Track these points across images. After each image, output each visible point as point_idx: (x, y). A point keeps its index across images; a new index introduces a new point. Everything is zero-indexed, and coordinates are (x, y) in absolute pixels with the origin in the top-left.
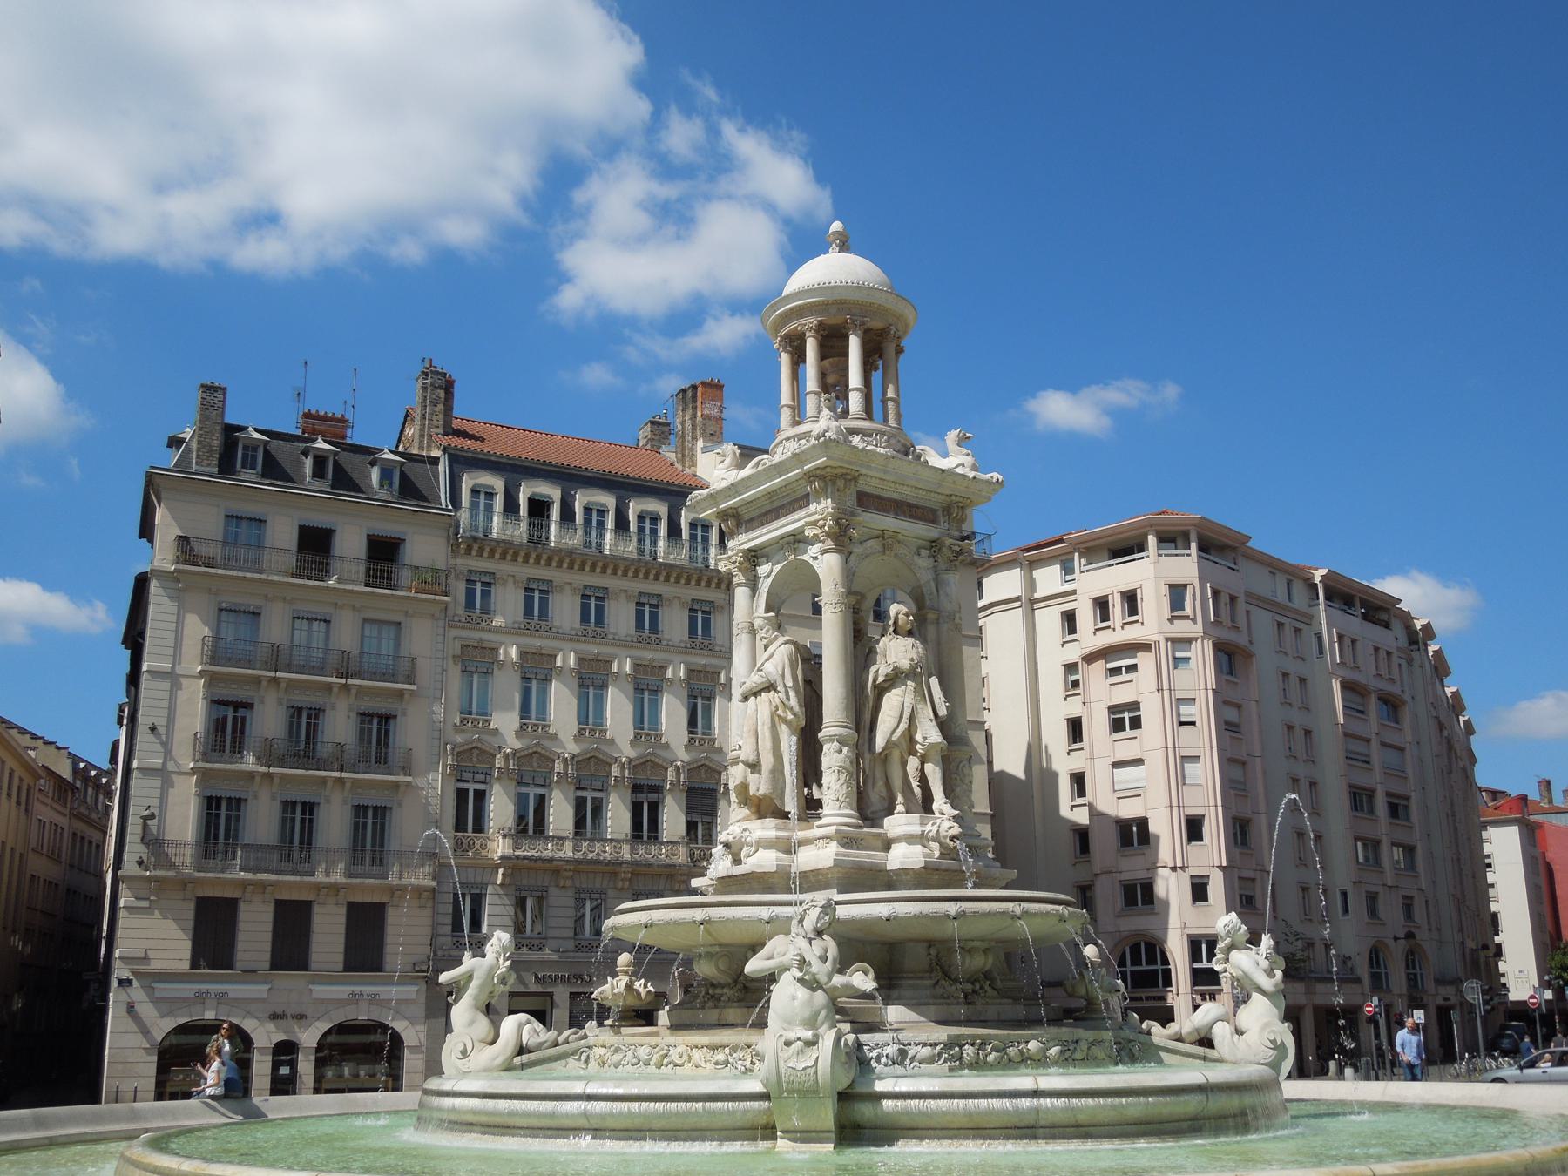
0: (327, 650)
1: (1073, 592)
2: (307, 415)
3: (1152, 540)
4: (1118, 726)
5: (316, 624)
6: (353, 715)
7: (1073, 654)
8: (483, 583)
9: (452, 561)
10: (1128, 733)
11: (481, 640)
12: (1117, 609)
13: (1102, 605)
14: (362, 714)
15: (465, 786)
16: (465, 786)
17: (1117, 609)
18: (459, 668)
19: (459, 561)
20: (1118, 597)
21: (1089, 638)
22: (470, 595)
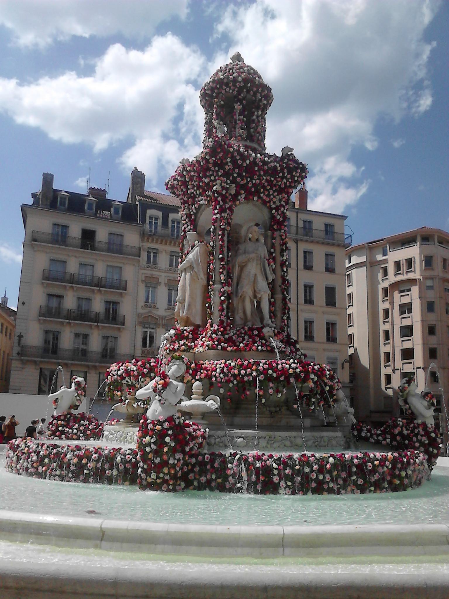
0: (93, 276)
1: (386, 260)
2: (90, 189)
3: (419, 238)
4: (402, 313)
5: (89, 267)
6: (103, 301)
7: (386, 284)
8: (154, 253)
9: (141, 244)
10: (407, 315)
11: (152, 275)
12: (404, 267)
13: (398, 264)
17: (404, 267)
18: (144, 285)
19: (144, 244)
20: (404, 261)
21: (392, 278)
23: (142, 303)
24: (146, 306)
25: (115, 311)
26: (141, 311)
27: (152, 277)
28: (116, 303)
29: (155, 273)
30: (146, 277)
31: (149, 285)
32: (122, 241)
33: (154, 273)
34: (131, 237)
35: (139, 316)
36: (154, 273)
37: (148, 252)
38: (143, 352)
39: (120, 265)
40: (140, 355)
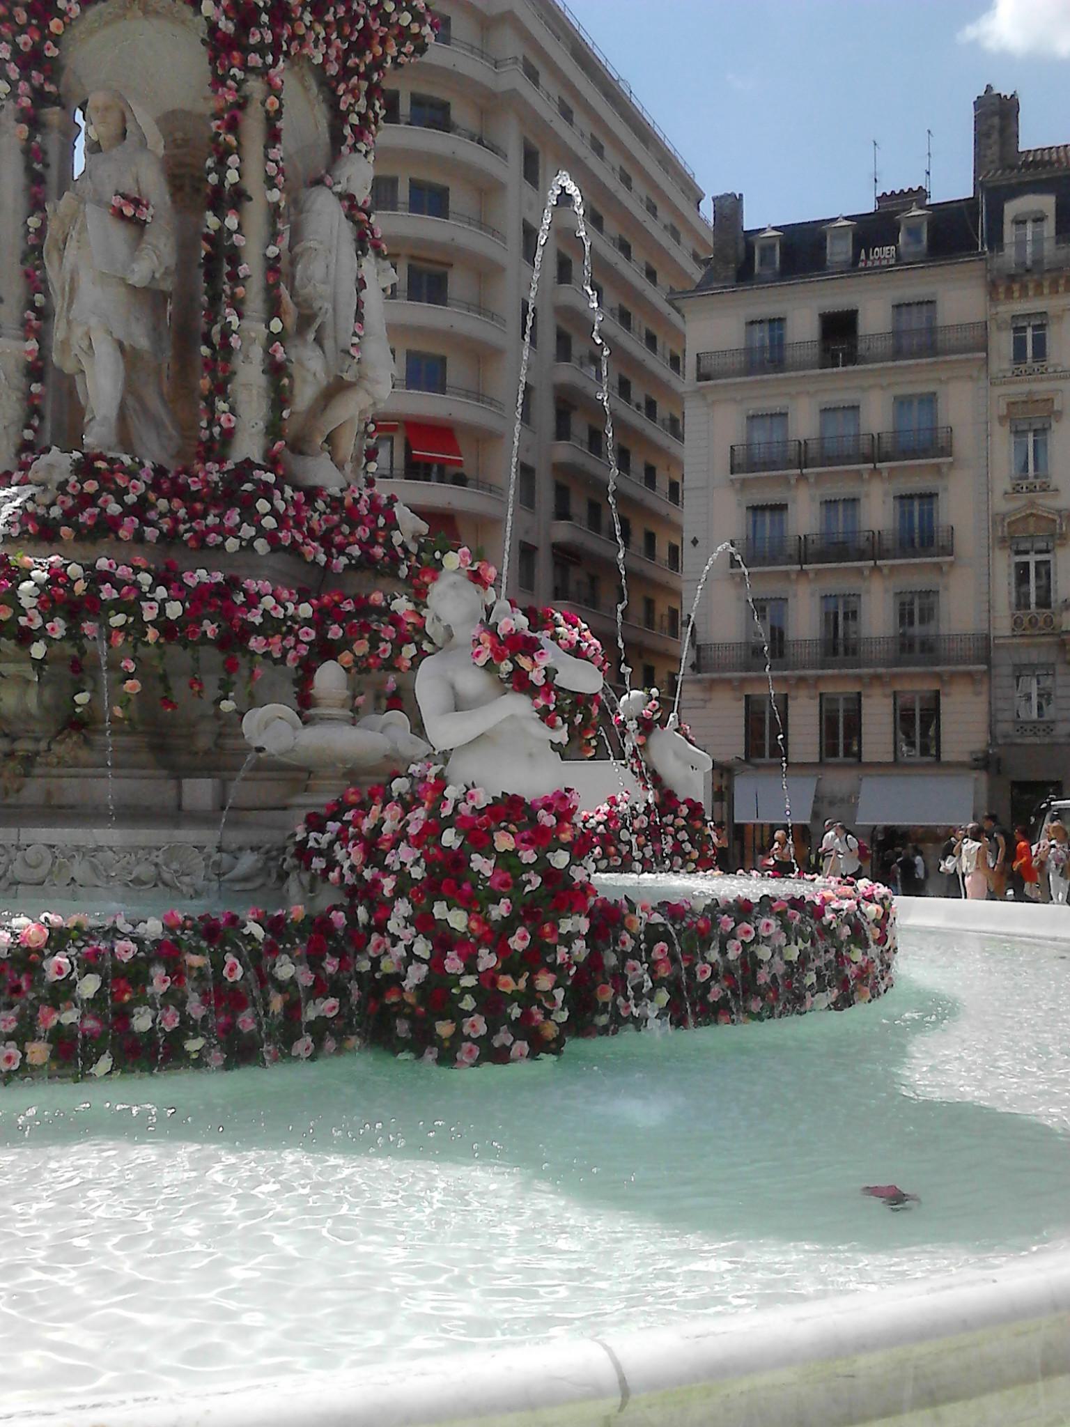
8: (1035, 328)
14: (901, 497)
15: (1024, 558)
16: (1024, 558)
19: (1001, 309)
22: (1019, 345)
23: (1003, 483)
24: (1017, 489)
25: (928, 518)
26: (1001, 505)
27: (1030, 401)
28: (930, 497)
29: (1041, 388)
30: (1011, 405)
31: (1025, 427)
32: (932, 318)
33: (1035, 387)
34: (959, 297)
35: (994, 523)
36: (1035, 387)
37: (1016, 330)
38: (1017, 622)
39: (931, 388)
40: (1008, 633)
